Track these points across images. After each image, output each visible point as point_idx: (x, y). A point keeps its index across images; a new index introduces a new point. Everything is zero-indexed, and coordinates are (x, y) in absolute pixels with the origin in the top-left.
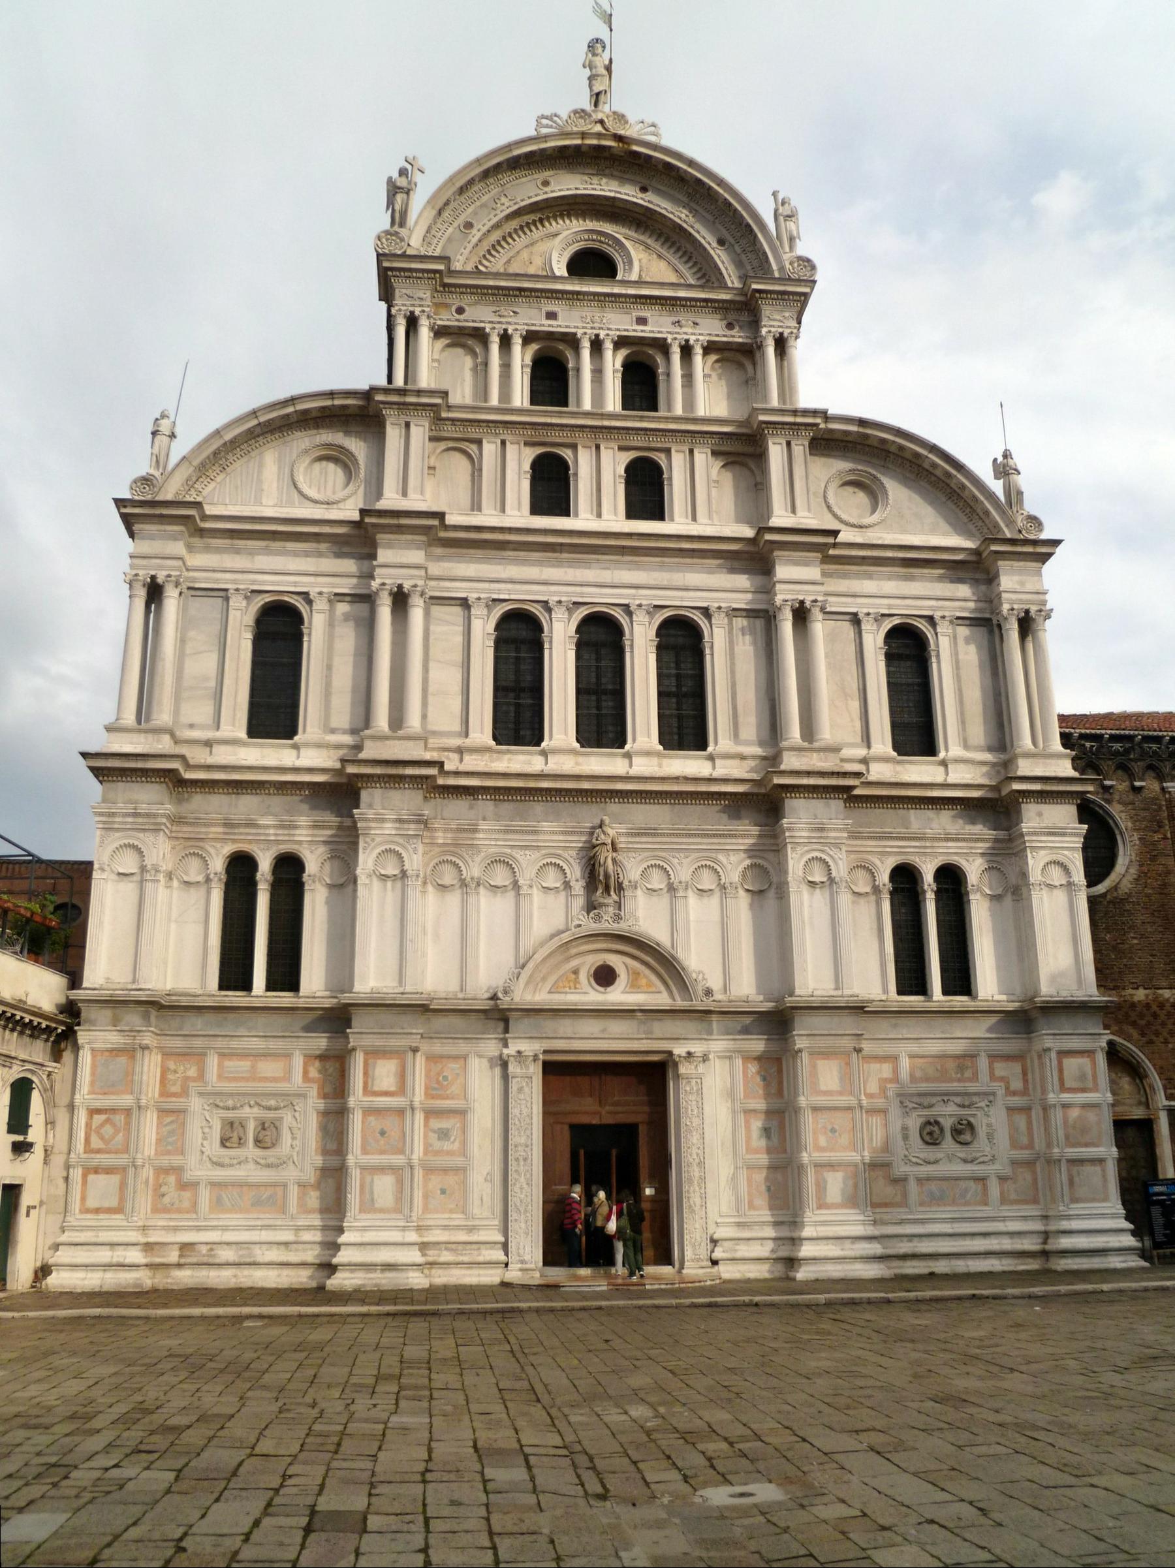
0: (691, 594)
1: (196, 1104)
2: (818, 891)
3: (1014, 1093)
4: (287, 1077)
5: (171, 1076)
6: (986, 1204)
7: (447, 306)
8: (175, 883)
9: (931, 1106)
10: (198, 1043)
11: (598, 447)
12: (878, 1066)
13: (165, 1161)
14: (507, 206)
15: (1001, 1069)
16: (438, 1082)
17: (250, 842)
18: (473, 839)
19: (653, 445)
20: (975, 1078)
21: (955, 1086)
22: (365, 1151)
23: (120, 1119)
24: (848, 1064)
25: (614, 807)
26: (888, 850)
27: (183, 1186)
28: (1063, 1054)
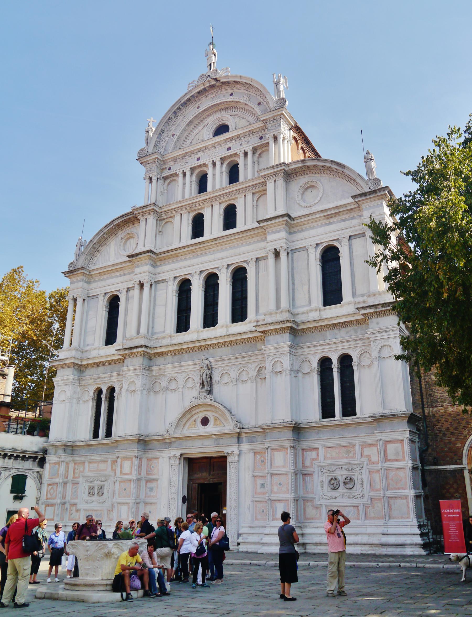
0: (242, 256)
1: (81, 480)
2: (279, 375)
3: (373, 463)
4: (106, 470)
5: (76, 471)
6: (358, 519)
7: (165, 168)
8: (81, 402)
9: (333, 471)
10: (83, 458)
11: (212, 205)
12: (311, 452)
13: (73, 502)
14: (186, 121)
15: (367, 451)
16: (151, 469)
17: (101, 384)
18: (164, 372)
19: (231, 198)
20: (354, 457)
21: (345, 461)
22: (119, 496)
23: (55, 486)
24: (287, 453)
25: (211, 351)
26: (317, 351)
27: (77, 511)
28: (385, 443)
